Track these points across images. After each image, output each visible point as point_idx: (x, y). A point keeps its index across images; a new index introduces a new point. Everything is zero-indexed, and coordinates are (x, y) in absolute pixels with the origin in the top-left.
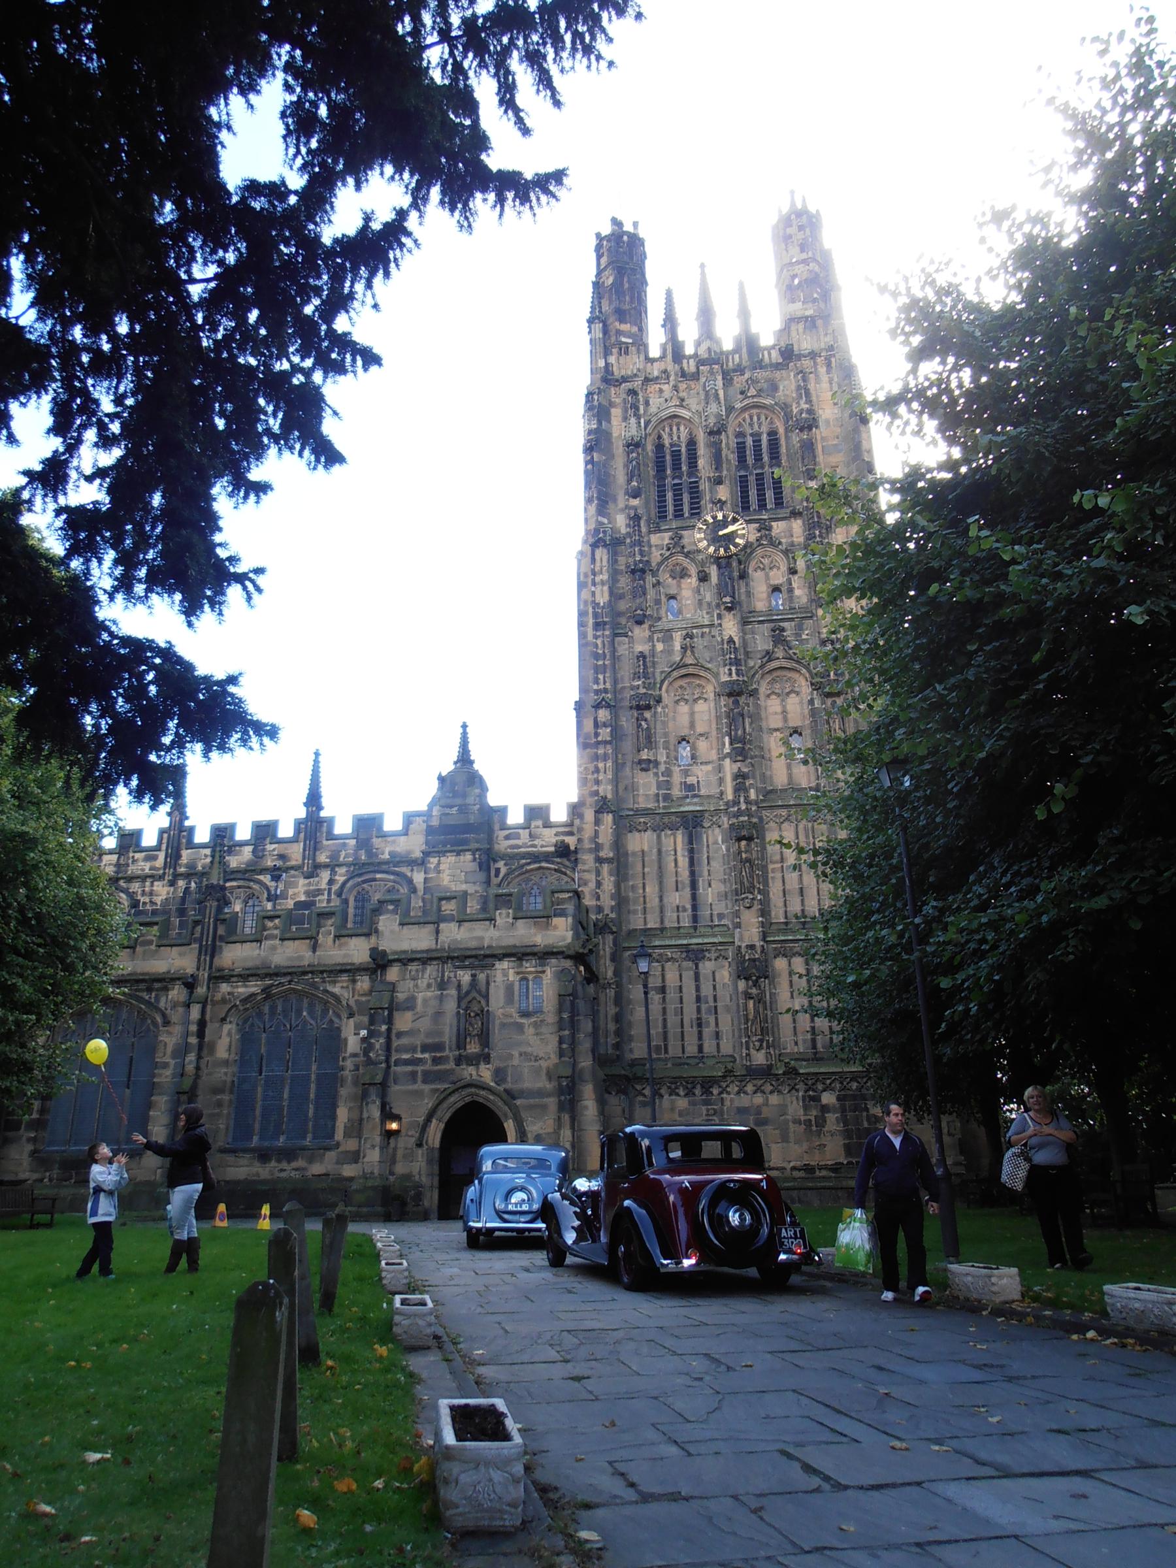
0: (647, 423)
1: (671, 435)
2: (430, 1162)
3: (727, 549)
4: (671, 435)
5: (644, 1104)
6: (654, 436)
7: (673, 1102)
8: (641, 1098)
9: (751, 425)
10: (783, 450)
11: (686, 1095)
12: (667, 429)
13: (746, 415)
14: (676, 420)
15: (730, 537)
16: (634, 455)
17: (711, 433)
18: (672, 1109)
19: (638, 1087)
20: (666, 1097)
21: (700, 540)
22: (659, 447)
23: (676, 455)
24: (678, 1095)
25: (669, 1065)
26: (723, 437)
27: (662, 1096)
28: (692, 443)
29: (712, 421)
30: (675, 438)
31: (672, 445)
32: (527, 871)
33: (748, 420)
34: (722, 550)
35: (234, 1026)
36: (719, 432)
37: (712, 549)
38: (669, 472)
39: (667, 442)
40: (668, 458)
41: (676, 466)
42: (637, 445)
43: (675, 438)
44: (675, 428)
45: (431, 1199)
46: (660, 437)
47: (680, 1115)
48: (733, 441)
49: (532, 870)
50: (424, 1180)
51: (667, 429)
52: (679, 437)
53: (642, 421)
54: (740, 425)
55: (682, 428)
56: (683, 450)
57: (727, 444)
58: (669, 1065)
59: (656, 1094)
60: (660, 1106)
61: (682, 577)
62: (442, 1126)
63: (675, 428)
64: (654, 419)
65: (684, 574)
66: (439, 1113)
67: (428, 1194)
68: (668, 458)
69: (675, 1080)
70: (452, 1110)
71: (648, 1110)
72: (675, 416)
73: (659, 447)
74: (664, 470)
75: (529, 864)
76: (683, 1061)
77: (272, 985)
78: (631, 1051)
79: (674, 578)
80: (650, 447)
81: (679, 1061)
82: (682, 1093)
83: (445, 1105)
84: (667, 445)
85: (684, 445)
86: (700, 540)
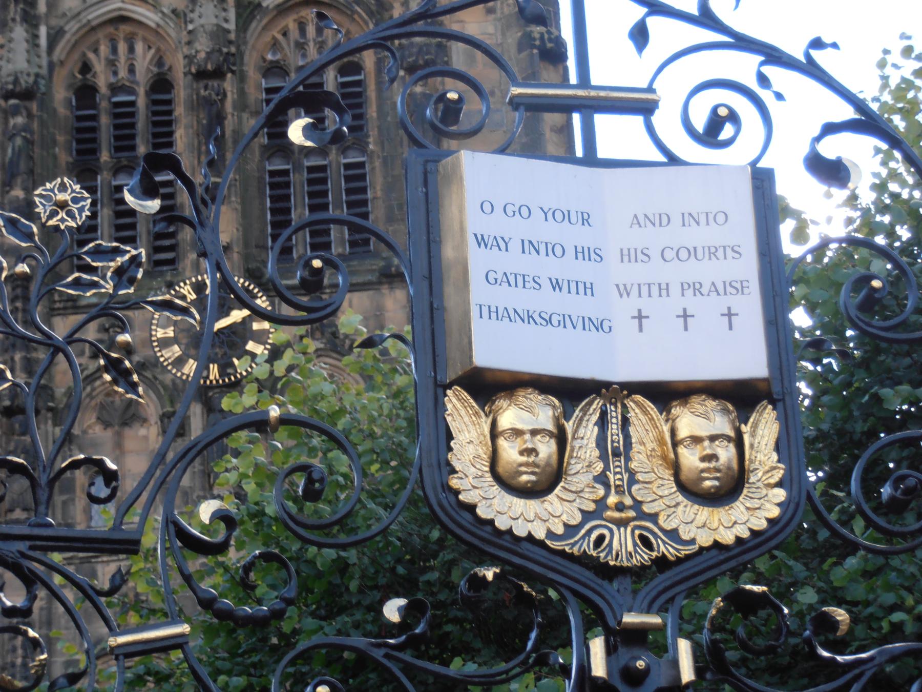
0: (55, 37)
1: (112, 64)
3: (226, 367)
4: (112, 64)
6: (73, 65)
9: (301, 46)
10: (372, 111)
12: (104, 49)
13: (290, 22)
14: (125, 28)
15: (235, 339)
16: (20, 120)
17: (201, 75)
21: (165, 343)
22: (85, 93)
23: (123, 115)
26: (229, 84)
28: (161, 84)
29: (203, 46)
30: (123, 73)
31: (115, 89)
33: (294, 33)
34: (214, 370)
36: (218, 74)
37: (191, 367)
38: (105, 156)
39: (102, 80)
40: (105, 120)
41: (124, 141)
42: (27, 95)
43: (123, 73)
44: (122, 47)
46: (86, 68)
48: (255, 94)
51: (104, 49)
52: (132, 70)
53: (43, 31)
54: (275, 45)
55: (139, 47)
56: (141, 102)
57: (242, 105)
61: (125, 423)
63: (122, 47)
64: (72, 27)
65: (130, 415)
68: (105, 120)
72: (123, 19)
73: (85, 93)
74: (94, 152)
79: (107, 425)
80: (61, 94)
84: (103, 89)
85: (141, 91)
86: (165, 343)
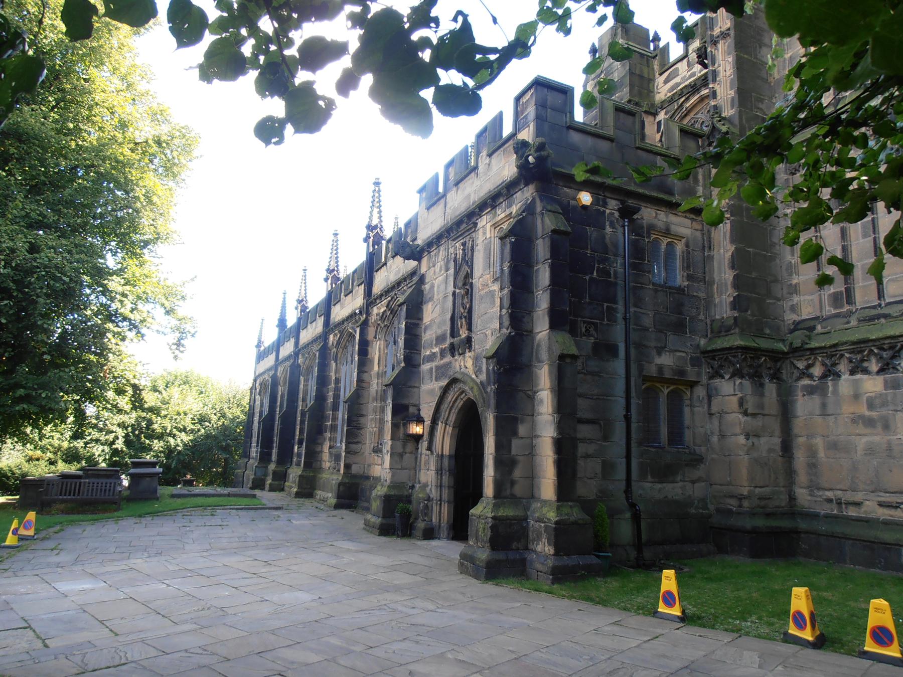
2: (439, 471)
5: (810, 391)
7: (856, 383)
8: (806, 382)
11: (881, 371)
18: (856, 396)
19: (801, 365)
20: (845, 377)
24: (866, 371)
25: (854, 323)
27: (838, 375)
32: (689, 112)
35: (382, 342)
45: (442, 514)
47: (871, 405)
49: (694, 106)
50: (434, 494)
58: (854, 323)
59: (831, 373)
60: (835, 392)
62: (449, 429)
66: (444, 414)
67: (435, 509)
69: (860, 346)
70: (455, 411)
71: (817, 399)
75: (687, 99)
76: (879, 311)
77: (389, 302)
78: (793, 309)
81: (874, 312)
82: (874, 366)
83: (445, 406)
